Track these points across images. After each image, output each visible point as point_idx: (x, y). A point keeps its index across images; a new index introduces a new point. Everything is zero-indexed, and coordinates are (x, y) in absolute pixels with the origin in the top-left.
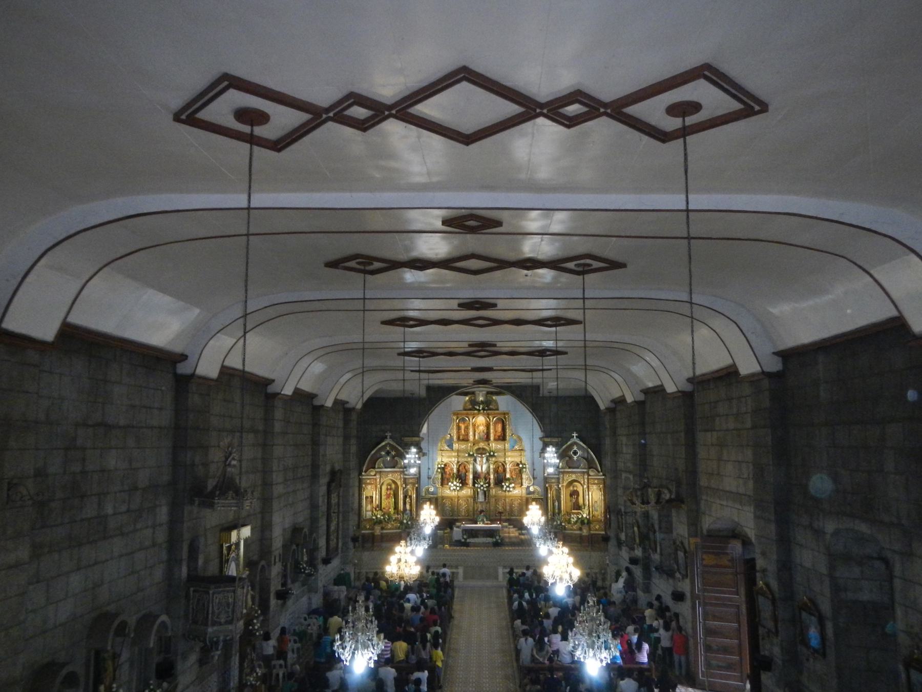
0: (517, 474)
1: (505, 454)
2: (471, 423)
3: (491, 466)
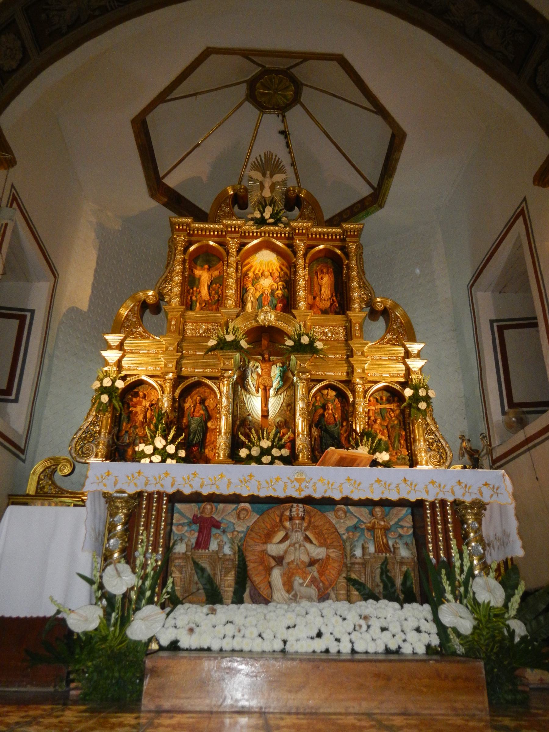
0: (389, 429)
1: (350, 354)
2: (232, 260)
3: (300, 392)
